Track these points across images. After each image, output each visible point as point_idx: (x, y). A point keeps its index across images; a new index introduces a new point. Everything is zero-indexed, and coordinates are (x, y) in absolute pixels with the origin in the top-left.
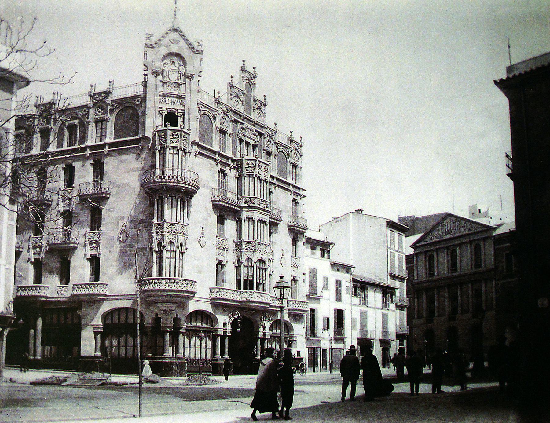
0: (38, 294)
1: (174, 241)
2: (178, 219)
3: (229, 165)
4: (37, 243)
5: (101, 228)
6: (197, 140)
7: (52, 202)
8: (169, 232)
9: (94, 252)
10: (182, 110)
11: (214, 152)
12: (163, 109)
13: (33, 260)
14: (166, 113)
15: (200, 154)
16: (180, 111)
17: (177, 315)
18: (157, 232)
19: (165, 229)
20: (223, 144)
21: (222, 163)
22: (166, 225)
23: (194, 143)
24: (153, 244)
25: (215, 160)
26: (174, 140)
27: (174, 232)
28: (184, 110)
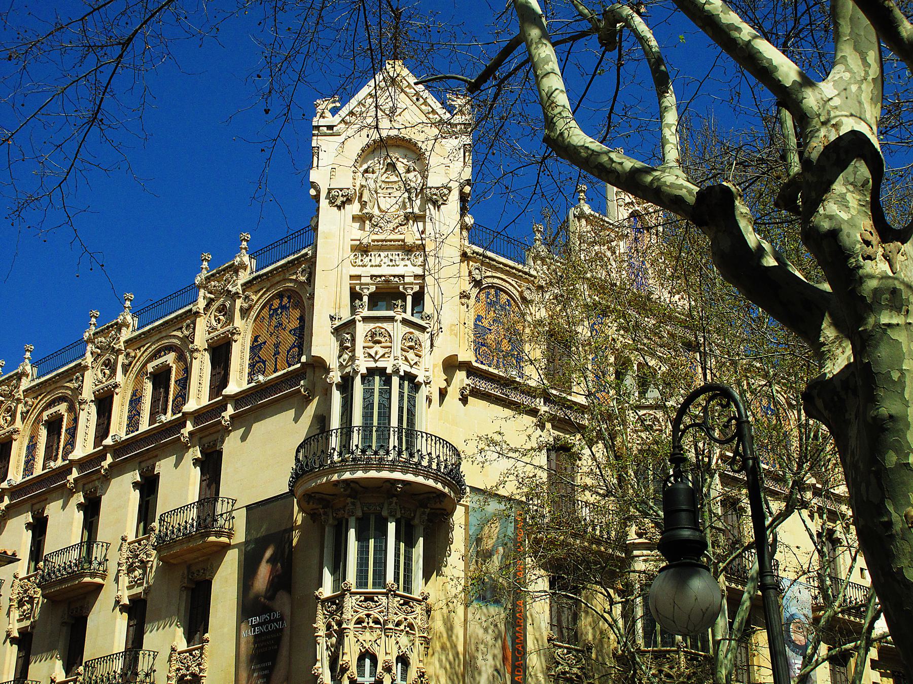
2: (390, 578)
3: (581, 429)
5: (206, 635)
6: (466, 355)
7: (104, 577)
8: (359, 621)
10: (416, 276)
11: (530, 392)
12: (364, 280)
14: (373, 289)
15: (476, 393)
16: (411, 280)
18: (329, 627)
19: (348, 614)
20: (558, 372)
21: (561, 424)
22: (350, 602)
23: (451, 365)
24: (318, 664)
25: (533, 412)
26: (378, 349)
27: (376, 621)
28: (423, 277)
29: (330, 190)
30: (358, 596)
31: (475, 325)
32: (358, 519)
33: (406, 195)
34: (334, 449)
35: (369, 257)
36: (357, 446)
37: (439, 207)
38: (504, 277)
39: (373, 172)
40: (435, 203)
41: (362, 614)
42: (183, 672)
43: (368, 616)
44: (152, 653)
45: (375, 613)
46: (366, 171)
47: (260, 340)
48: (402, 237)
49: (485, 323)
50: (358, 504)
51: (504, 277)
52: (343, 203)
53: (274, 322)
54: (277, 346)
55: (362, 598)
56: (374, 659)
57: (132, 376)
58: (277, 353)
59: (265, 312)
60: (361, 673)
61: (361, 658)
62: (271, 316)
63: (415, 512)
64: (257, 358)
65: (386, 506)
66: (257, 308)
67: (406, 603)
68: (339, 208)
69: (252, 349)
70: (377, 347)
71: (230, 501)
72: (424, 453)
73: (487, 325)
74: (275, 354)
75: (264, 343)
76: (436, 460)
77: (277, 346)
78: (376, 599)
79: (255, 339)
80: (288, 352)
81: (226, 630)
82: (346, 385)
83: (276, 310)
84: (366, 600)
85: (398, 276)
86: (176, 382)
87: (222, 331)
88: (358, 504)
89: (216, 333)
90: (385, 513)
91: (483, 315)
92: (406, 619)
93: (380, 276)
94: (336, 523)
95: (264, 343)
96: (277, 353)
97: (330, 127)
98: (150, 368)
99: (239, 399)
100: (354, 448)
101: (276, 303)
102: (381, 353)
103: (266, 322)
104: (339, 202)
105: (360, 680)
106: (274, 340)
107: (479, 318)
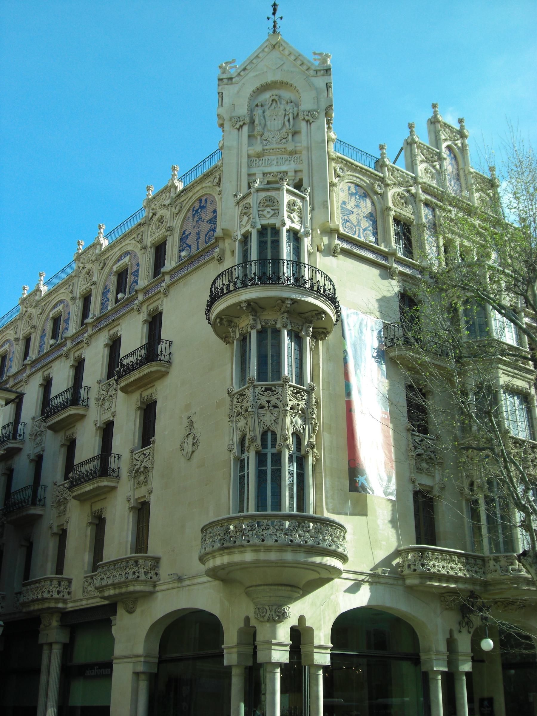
0: (46, 595)
1: (273, 428)
4: (62, 494)
9: (142, 492)
13: (55, 530)
17: (302, 619)
27: (275, 407)
29: (231, 119)
30: (260, 388)
31: (342, 208)
32: (259, 333)
33: (287, 118)
34: (237, 278)
35: (261, 162)
36: (255, 274)
37: (310, 124)
38: (361, 177)
39: (262, 106)
40: (307, 121)
41: (263, 400)
42: (138, 466)
43: (268, 402)
44: (117, 456)
45: (274, 400)
46: (257, 106)
47: (187, 233)
48: (284, 146)
49: (349, 207)
50: (258, 321)
51: (361, 177)
52: (241, 126)
53: (196, 218)
54: (198, 234)
55: (263, 389)
56: (274, 434)
57: (104, 277)
58: (198, 238)
59: (190, 214)
60: (264, 446)
61: (264, 435)
62: (194, 215)
63: (302, 326)
64: (185, 245)
65: (279, 321)
66: (184, 211)
67: (297, 393)
68: (238, 129)
69: (181, 240)
70: (268, 209)
71: (168, 342)
72: (307, 278)
73: (350, 208)
74: (197, 239)
75: (190, 234)
76: (316, 285)
77: (198, 234)
78: (273, 389)
79: (184, 233)
80: (206, 235)
81: (166, 433)
82: (246, 238)
83: (197, 210)
84: (267, 389)
85: (283, 172)
86: (132, 274)
87: (161, 232)
88: (258, 321)
89: (157, 234)
90: (278, 326)
91: (347, 201)
92: (298, 405)
93: (270, 173)
94: (242, 338)
95: (190, 234)
96: (198, 238)
97: (231, 79)
98: (115, 269)
99: (173, 272)
100: (253, 276)
101: (197, 205)
102: (272, 212)
103: (191, 220)
104: (238, 126)
105: (265, 451)
106: (196, 230)
107: (344, 203)
